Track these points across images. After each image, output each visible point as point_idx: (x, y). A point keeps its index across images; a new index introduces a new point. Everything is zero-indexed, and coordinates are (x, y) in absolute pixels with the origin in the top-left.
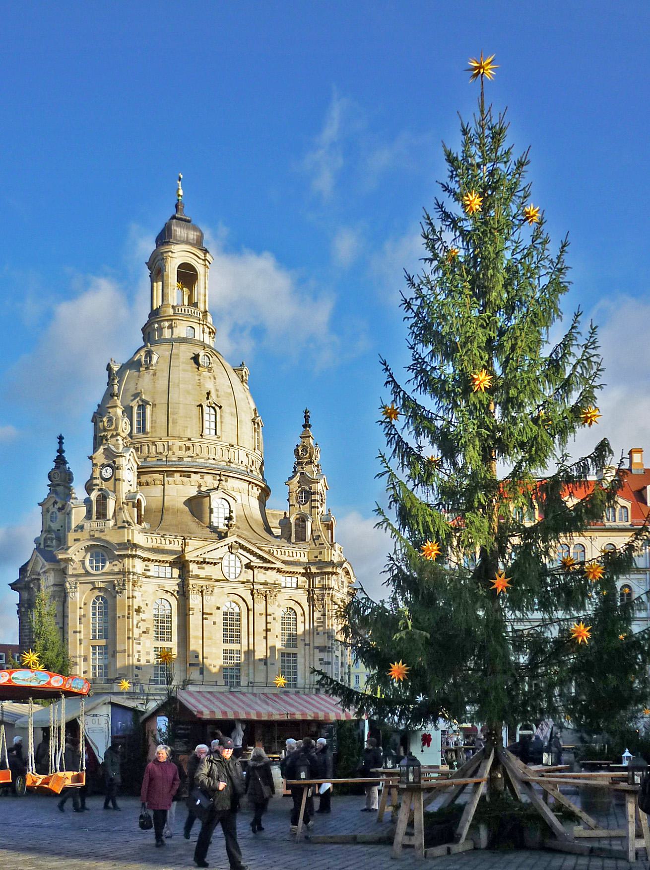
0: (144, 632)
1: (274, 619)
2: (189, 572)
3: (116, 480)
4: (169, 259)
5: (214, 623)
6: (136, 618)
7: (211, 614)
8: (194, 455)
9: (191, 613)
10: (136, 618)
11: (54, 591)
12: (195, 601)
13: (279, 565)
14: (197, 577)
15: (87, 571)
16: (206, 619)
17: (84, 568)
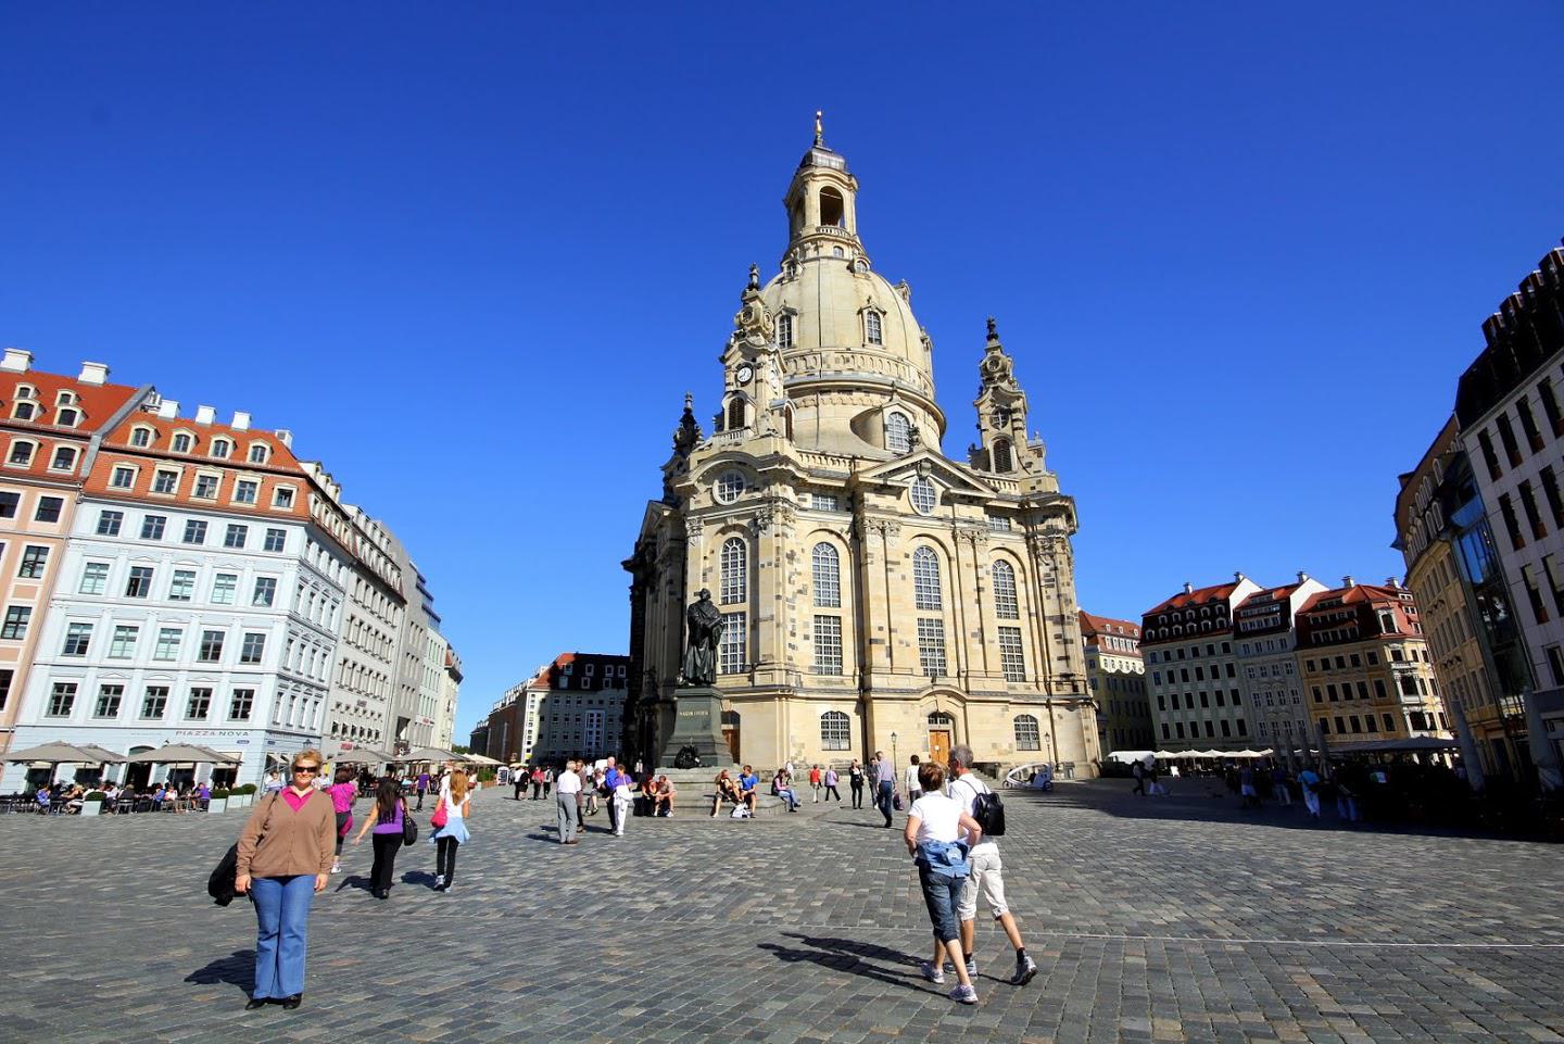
0: (800, 592)
1: (988, 573)
2: (863, 501)
3: (756, 382)
4: (811, 183)
5: (904, 578)
6: (788, 568)
7: (898, 563)
8: (856, 369)
9: (869, 560)
10: (788, 568)
11: (671, 548)
12: (873, 542)
13: (987, 493)
14: (875, 508)
15: (716, 503)
16: (891, 570)
17: (712, 498)
